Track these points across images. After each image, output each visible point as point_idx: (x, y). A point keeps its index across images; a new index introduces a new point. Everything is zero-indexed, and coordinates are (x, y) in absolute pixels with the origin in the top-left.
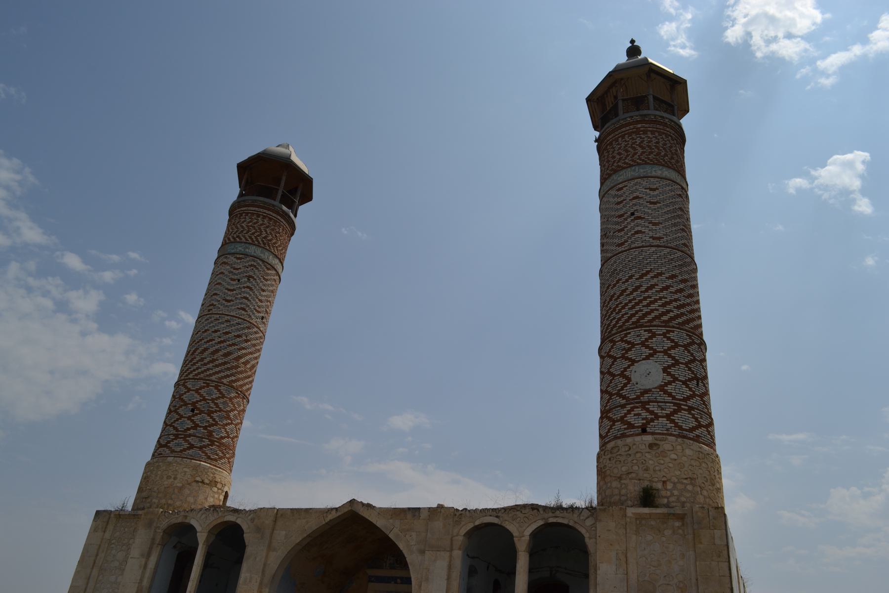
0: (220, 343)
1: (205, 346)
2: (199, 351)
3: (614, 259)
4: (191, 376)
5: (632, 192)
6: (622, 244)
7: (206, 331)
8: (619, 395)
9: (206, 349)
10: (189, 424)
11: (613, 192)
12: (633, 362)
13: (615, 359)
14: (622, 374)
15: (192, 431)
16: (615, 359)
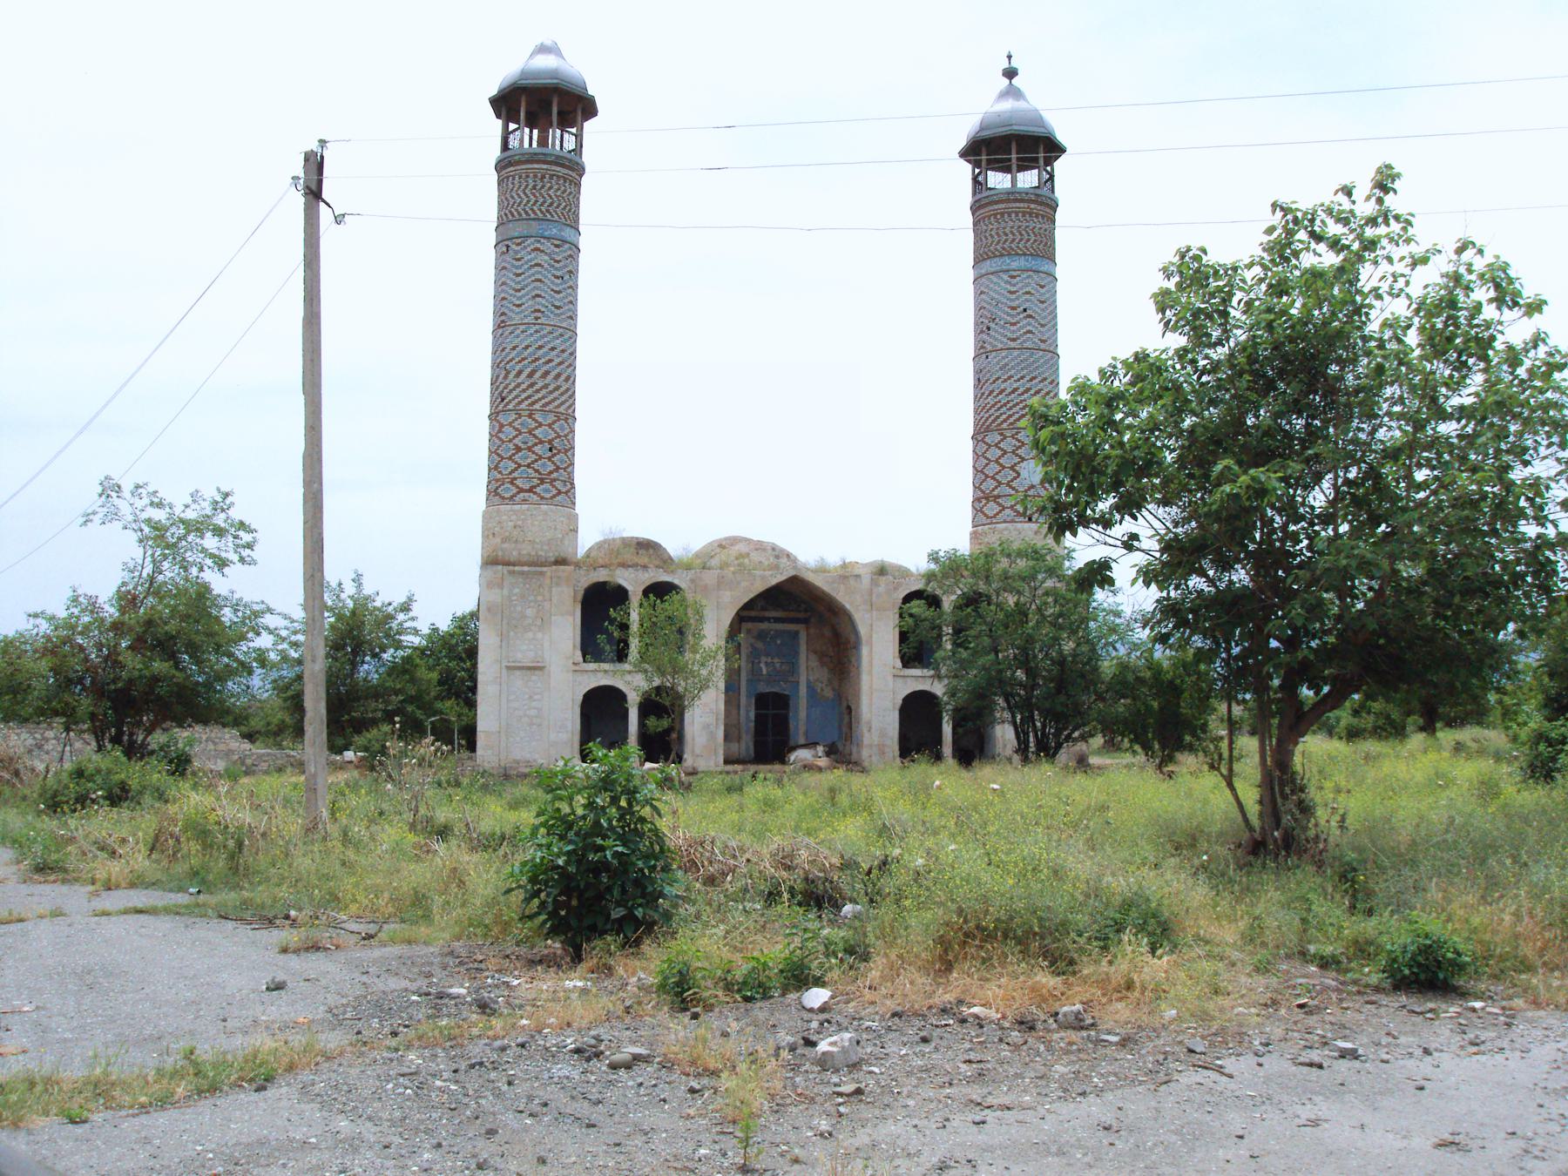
0: (560, 363)
1: (546, 368)
2: (538, 374)
3: (1004, 353)
4: (537, 406)
5: (1028, 285)
6: (1014, 340)
7: (540, 347)
8: (1008, 484)
9: (547, 373)
10: (553, 468)
11: (1006, 277)
12: (1023, 459)
13: (1005, 452)
14: (1012, 468)
15: (555, 475)
16: (1005, 452)
